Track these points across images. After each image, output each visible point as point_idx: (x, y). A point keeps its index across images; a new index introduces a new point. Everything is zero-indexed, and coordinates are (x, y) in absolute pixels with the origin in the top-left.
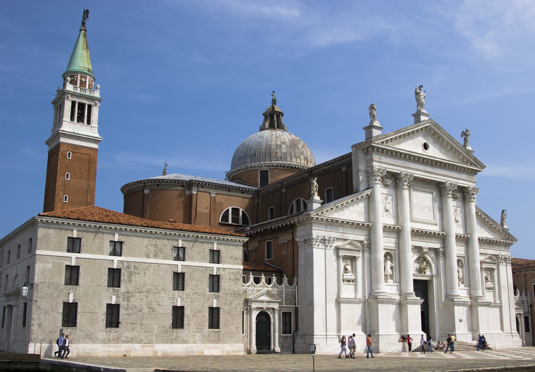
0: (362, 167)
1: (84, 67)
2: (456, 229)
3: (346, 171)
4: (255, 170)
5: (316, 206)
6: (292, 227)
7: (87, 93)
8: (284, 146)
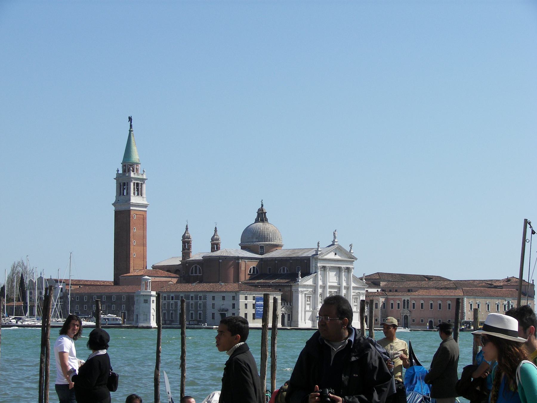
1: (137, 159)
2: (344, 284)
3: (306, 262)
5: (300, 280)
6: (291, 286)
7: (140, 177)
8: (270, 234)
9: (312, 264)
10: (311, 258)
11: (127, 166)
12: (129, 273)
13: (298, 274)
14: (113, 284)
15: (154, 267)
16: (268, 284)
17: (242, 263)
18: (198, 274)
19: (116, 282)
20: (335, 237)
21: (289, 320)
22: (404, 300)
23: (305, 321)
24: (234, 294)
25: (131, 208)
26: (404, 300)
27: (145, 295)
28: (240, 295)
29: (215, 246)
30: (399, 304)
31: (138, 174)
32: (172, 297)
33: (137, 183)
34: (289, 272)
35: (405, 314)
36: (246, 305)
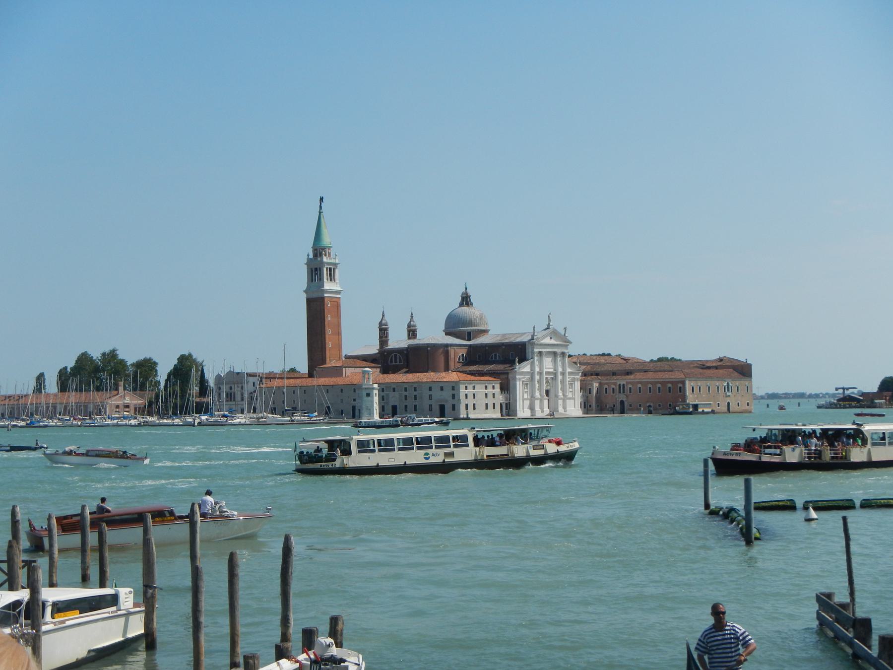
0: (530, 350)
2: (560, 370)
3: (521, 348)
4: (464, 331)
5: (517, 367)
6: (507, 374)
7: (332, 261)
8: (477, 319)
9: (529, 350)
10: (527, 344)
11: (318, 251)
12: (325, 364)
13: (515, 360)
14: (307, 376)
15: (347, 357)
16: (481, 372)
17: (452, 351)
18: (398, 363)
19: (311, 375)
20: (550, 320)
21: (506, 409)
22: (620, 385)
23: (523, 409)
24: (453, 384)
25: (325, 295)
26: (620, 385)
27: (368, 388)
28: (461, 385)
29: (412, 333)
30: (613, 389)
31: (330, 258)
32: (383, 390)
33: (330, 268)
34: (502, 359)
35: (621, 399)
36: (466, 395)
